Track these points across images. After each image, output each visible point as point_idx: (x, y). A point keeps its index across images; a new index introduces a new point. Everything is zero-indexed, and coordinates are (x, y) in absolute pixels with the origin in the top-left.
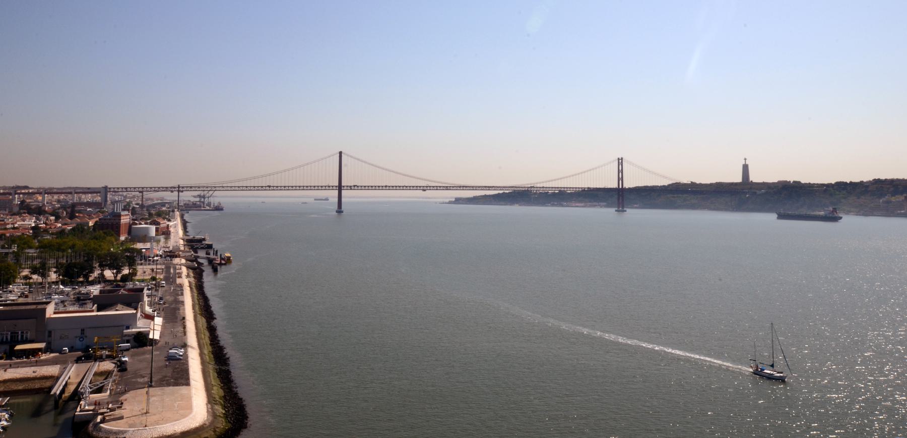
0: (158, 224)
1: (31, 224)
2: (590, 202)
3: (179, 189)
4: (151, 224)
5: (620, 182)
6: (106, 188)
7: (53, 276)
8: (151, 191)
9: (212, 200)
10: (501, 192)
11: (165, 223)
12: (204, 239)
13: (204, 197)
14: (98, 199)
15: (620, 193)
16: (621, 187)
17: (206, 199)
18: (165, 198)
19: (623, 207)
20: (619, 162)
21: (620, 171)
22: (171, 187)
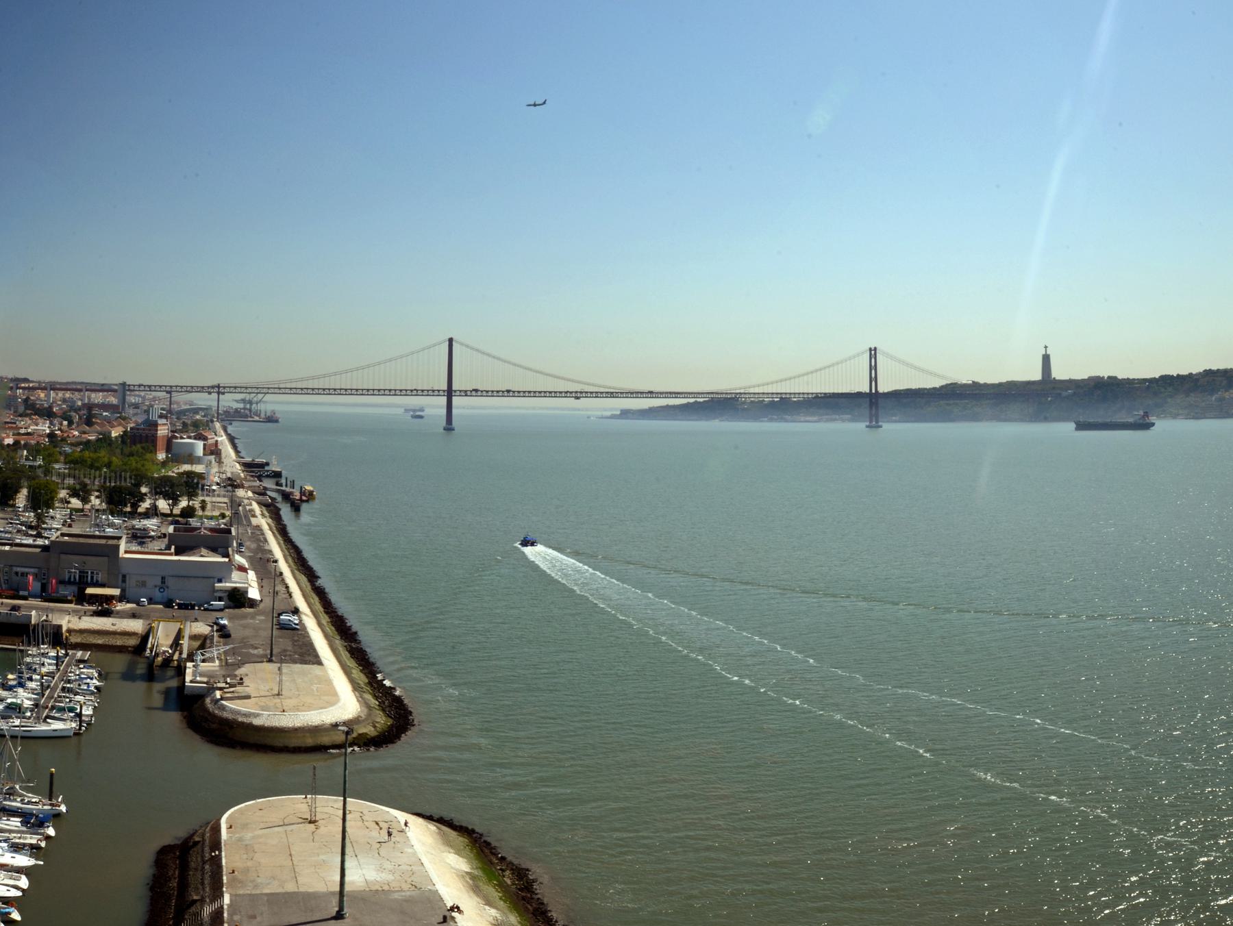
0: (205, 439)
1: (45, 430)
2: (827, 414)
3: (219, 389)
4: (195, 439)
5: (873, 383)
6: (124, 384)
7: (95, 501)
8: (182, 392)
9: (262, 407)
10: (692, 400)
11: (213, 438)
12: (267, 464)
13: (250, 402)
14: (113, 400)
15: (873, 400)
16: (874, 391)
17: (254, 405)
18: (195, 402)
19: (877, 422)
20: (871, 354)
21: (873, 368)
22: (208, 387)
